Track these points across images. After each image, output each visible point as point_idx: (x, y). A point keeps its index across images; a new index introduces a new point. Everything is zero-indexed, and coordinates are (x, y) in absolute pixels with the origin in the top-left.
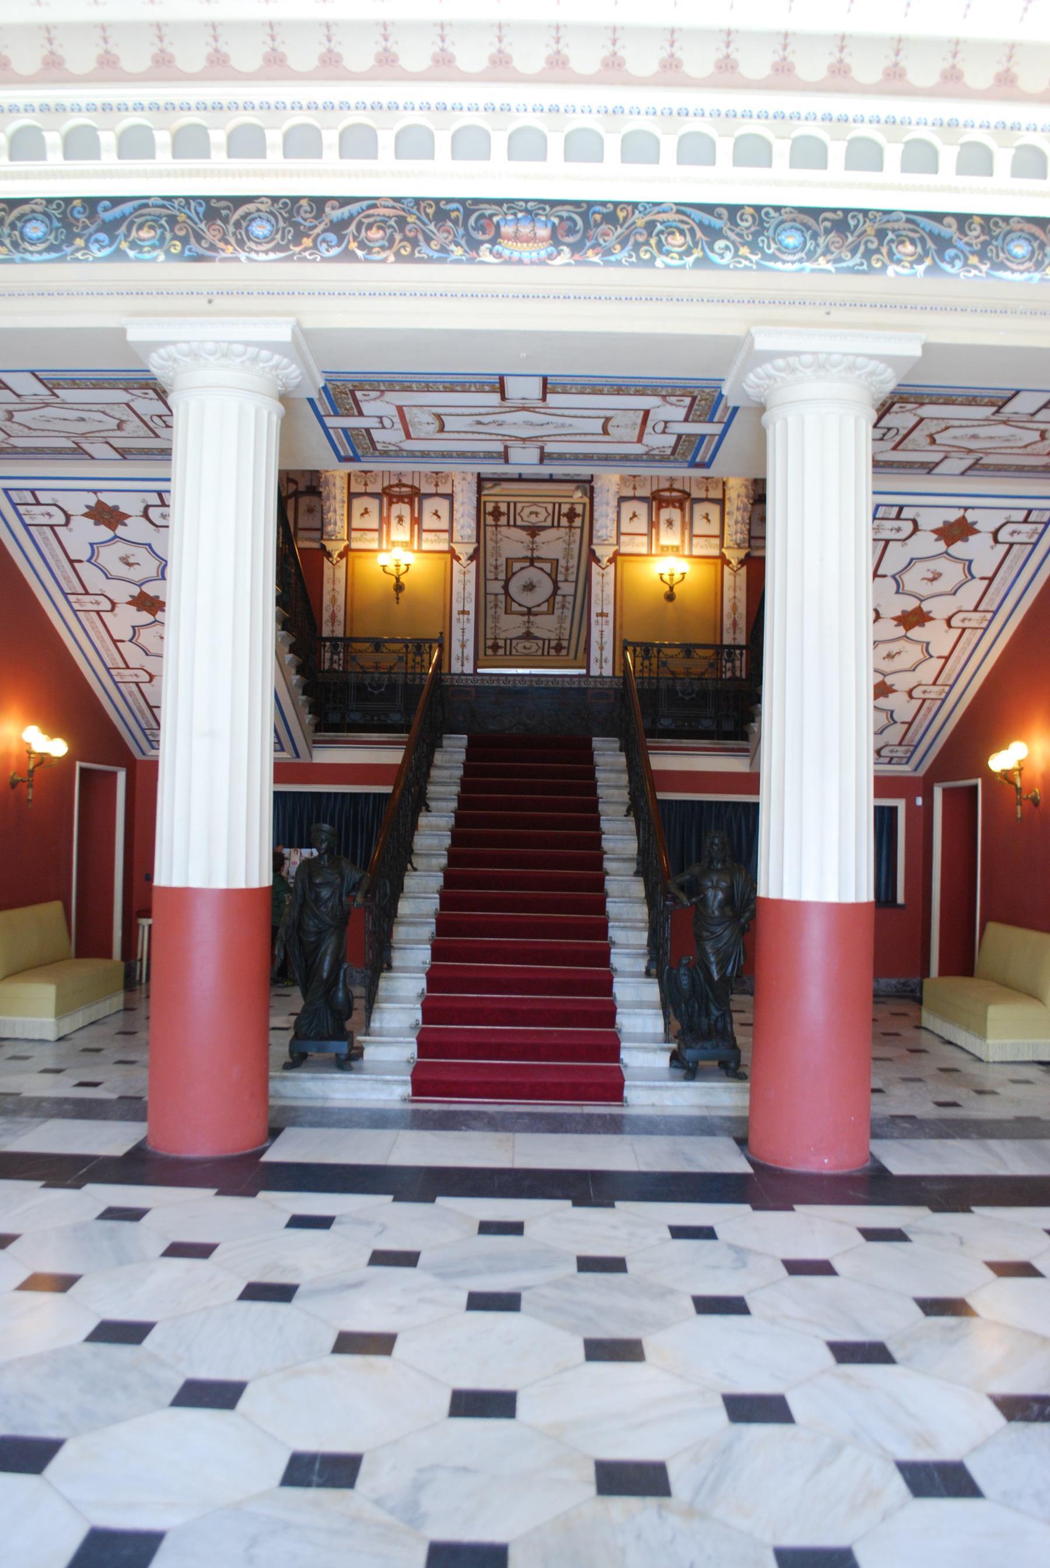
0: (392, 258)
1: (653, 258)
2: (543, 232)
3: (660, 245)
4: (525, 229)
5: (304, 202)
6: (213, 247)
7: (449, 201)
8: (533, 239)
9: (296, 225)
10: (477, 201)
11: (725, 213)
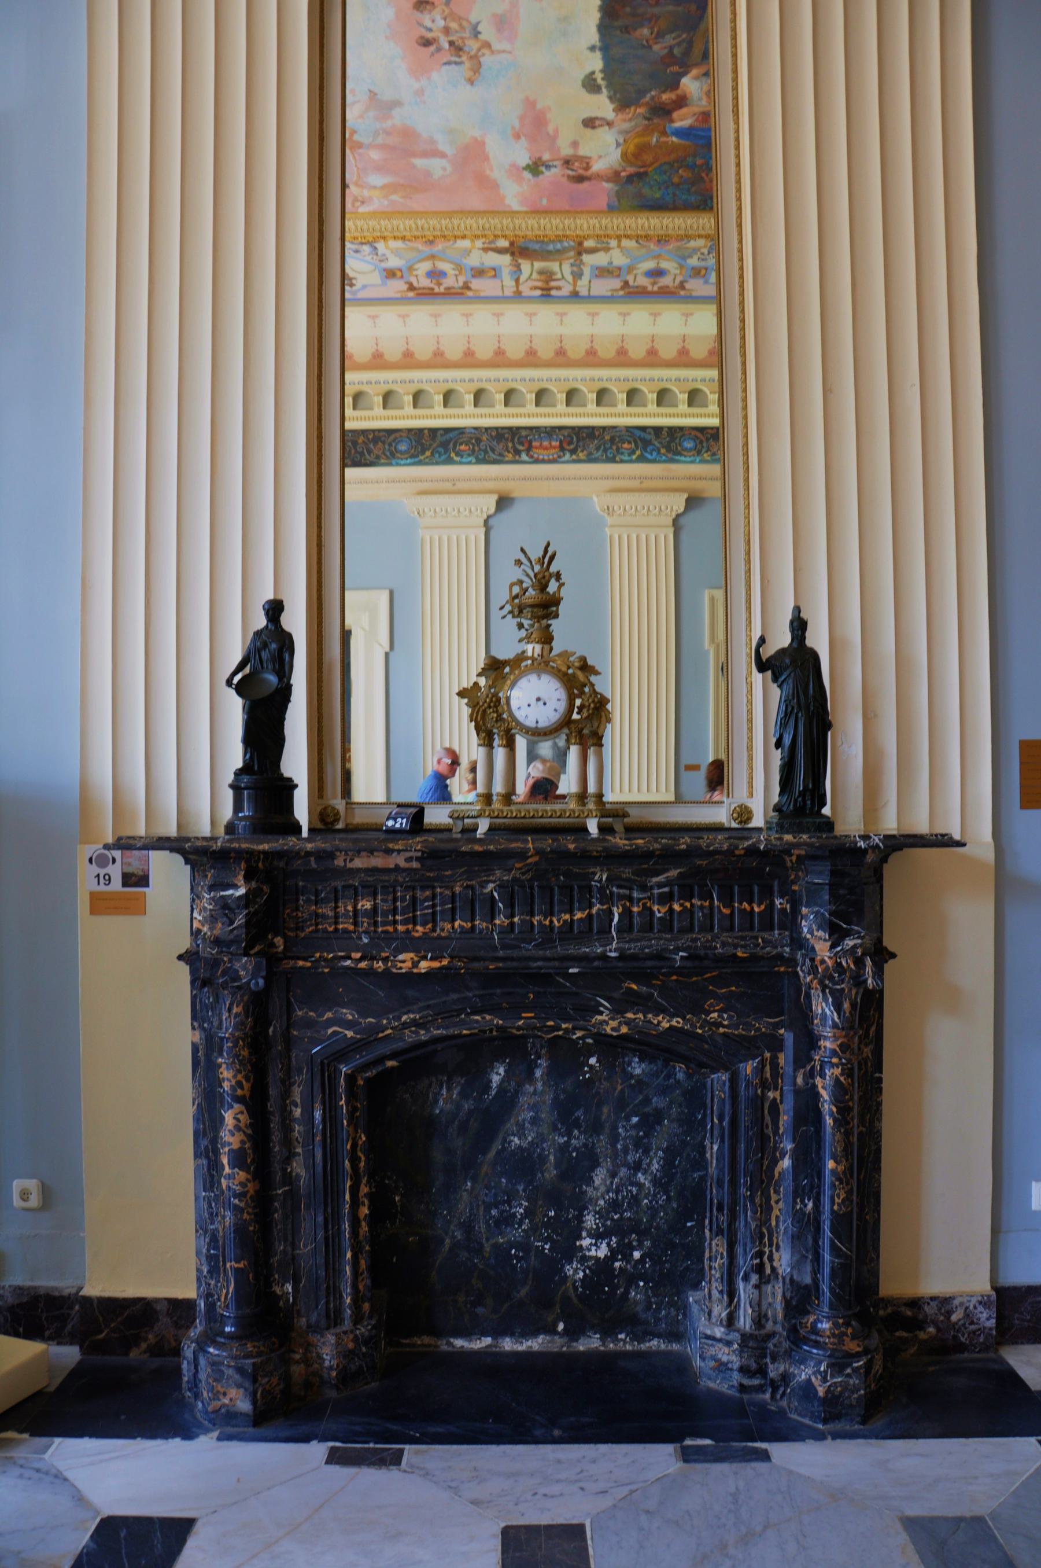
0: (474, 460)
1: (614, 457)
2: (555, 443)
3: (618, 449)
4: (546, 443)
5: (426, 431)
6: (378, 457)
7: (503, 428)
8: (552, 447)
9: (422, 445)
10: (519, 428)
11: (651, 431)
